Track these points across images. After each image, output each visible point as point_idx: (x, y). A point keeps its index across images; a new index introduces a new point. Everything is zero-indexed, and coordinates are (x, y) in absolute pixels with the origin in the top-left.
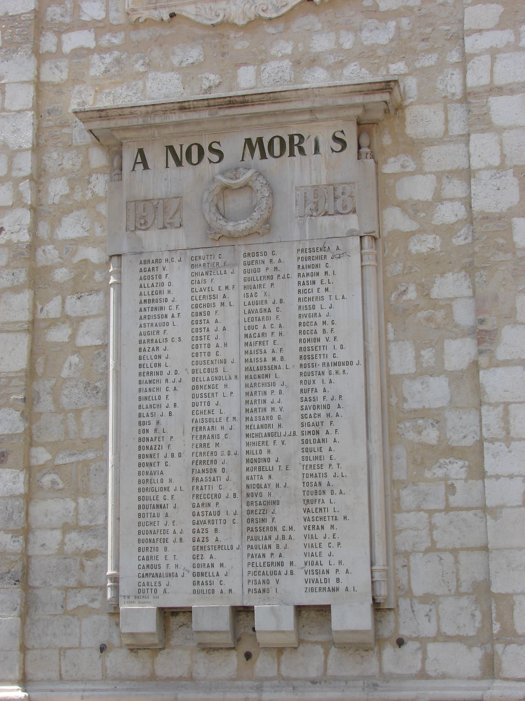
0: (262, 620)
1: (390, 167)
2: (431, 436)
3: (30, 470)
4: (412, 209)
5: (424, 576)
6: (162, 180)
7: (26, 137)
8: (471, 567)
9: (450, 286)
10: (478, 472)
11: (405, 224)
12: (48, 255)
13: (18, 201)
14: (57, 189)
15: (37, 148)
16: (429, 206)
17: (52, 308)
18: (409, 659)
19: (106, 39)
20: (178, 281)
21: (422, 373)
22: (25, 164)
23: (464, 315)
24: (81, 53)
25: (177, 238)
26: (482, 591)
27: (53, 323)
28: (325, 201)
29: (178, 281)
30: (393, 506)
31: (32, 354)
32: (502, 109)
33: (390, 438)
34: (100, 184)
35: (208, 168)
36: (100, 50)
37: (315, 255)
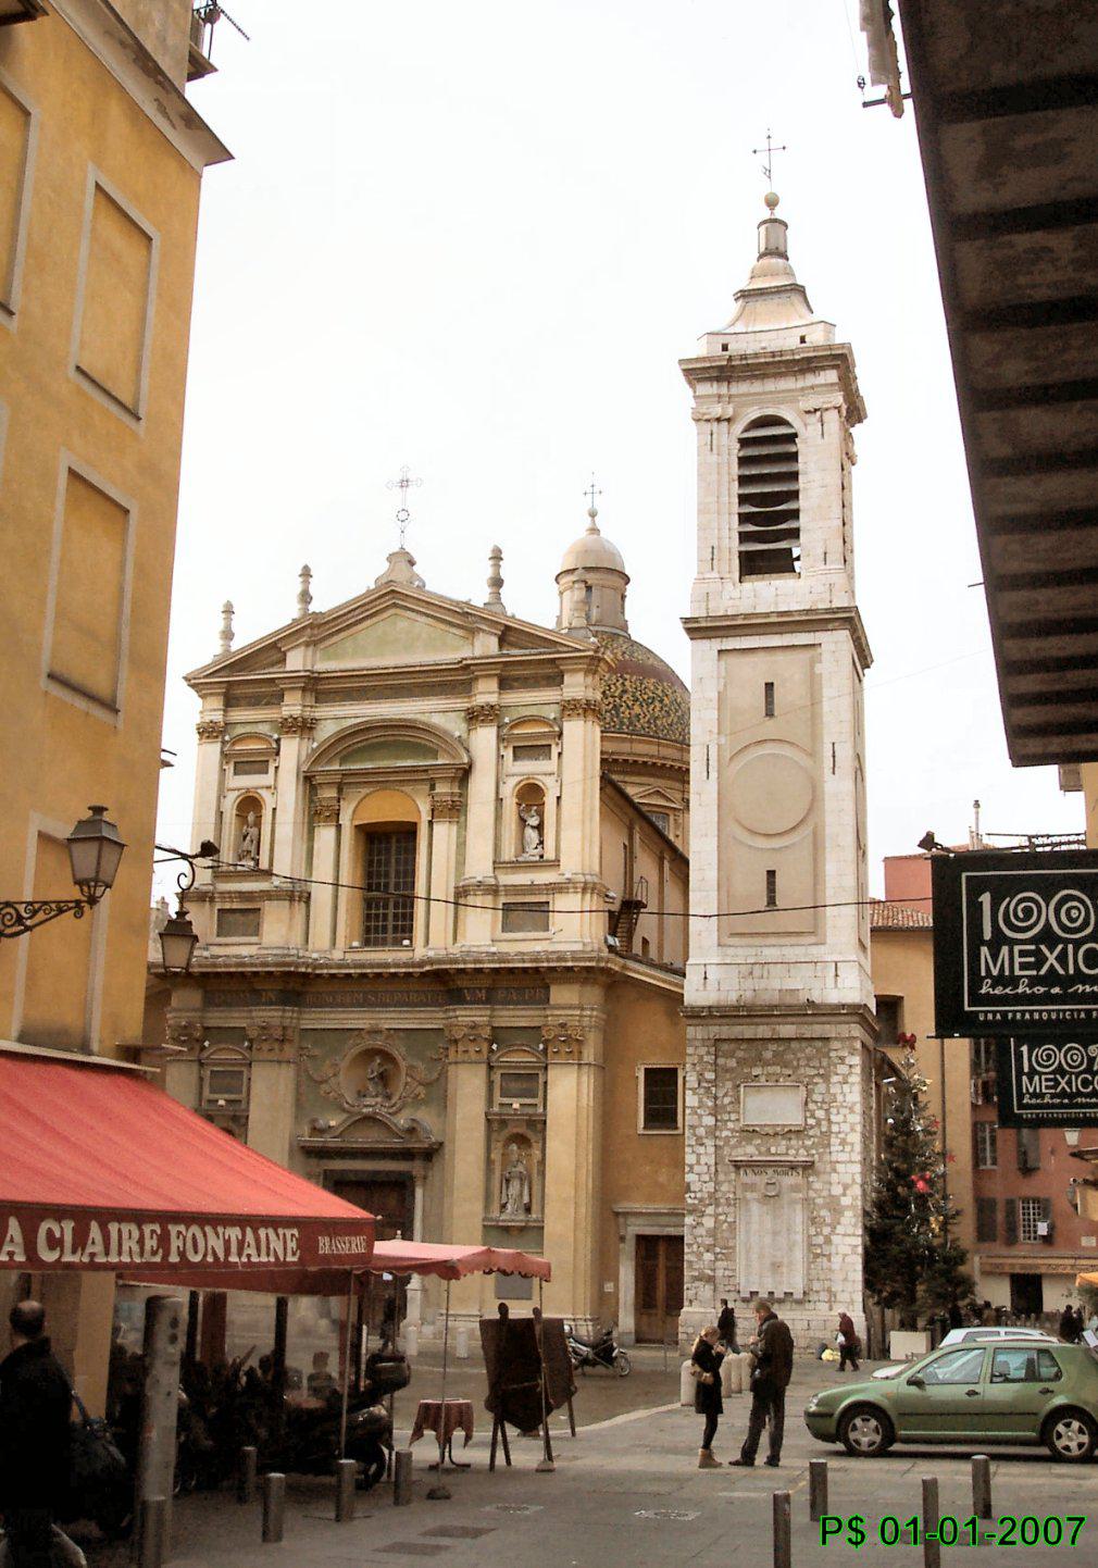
0: (776, 1296)
1: (811, 1179)
2: (819, 1251)
3: (716, 1254)
4: (816, 1191)
5: (816, 1286)
6: (749, 1177)
8: (827, 1284)
9: (824, 1213)
10: (829, 1260)
11: (815, 1195)
13: (711, 1180)
14: (721, 1177)
15: (716, 1164)
16: (821, 1191)
17: (720, 1210)
18: (811, 1306)
20: (755, 1207)
21: (817, 1234)
22: (713, 1169)
24: (727, 1136)
25: (755, 1195)
26: (829, 1290)
27: (721, 1214)
28: (795, 1188)
29: (755, 1207)
30: (809, 1269)
31: (715, 1222)
32: (840, 1167)
33: (809, 1251)
34: (733, 1176)
36: (734, 1137)
37: (793, 1202)
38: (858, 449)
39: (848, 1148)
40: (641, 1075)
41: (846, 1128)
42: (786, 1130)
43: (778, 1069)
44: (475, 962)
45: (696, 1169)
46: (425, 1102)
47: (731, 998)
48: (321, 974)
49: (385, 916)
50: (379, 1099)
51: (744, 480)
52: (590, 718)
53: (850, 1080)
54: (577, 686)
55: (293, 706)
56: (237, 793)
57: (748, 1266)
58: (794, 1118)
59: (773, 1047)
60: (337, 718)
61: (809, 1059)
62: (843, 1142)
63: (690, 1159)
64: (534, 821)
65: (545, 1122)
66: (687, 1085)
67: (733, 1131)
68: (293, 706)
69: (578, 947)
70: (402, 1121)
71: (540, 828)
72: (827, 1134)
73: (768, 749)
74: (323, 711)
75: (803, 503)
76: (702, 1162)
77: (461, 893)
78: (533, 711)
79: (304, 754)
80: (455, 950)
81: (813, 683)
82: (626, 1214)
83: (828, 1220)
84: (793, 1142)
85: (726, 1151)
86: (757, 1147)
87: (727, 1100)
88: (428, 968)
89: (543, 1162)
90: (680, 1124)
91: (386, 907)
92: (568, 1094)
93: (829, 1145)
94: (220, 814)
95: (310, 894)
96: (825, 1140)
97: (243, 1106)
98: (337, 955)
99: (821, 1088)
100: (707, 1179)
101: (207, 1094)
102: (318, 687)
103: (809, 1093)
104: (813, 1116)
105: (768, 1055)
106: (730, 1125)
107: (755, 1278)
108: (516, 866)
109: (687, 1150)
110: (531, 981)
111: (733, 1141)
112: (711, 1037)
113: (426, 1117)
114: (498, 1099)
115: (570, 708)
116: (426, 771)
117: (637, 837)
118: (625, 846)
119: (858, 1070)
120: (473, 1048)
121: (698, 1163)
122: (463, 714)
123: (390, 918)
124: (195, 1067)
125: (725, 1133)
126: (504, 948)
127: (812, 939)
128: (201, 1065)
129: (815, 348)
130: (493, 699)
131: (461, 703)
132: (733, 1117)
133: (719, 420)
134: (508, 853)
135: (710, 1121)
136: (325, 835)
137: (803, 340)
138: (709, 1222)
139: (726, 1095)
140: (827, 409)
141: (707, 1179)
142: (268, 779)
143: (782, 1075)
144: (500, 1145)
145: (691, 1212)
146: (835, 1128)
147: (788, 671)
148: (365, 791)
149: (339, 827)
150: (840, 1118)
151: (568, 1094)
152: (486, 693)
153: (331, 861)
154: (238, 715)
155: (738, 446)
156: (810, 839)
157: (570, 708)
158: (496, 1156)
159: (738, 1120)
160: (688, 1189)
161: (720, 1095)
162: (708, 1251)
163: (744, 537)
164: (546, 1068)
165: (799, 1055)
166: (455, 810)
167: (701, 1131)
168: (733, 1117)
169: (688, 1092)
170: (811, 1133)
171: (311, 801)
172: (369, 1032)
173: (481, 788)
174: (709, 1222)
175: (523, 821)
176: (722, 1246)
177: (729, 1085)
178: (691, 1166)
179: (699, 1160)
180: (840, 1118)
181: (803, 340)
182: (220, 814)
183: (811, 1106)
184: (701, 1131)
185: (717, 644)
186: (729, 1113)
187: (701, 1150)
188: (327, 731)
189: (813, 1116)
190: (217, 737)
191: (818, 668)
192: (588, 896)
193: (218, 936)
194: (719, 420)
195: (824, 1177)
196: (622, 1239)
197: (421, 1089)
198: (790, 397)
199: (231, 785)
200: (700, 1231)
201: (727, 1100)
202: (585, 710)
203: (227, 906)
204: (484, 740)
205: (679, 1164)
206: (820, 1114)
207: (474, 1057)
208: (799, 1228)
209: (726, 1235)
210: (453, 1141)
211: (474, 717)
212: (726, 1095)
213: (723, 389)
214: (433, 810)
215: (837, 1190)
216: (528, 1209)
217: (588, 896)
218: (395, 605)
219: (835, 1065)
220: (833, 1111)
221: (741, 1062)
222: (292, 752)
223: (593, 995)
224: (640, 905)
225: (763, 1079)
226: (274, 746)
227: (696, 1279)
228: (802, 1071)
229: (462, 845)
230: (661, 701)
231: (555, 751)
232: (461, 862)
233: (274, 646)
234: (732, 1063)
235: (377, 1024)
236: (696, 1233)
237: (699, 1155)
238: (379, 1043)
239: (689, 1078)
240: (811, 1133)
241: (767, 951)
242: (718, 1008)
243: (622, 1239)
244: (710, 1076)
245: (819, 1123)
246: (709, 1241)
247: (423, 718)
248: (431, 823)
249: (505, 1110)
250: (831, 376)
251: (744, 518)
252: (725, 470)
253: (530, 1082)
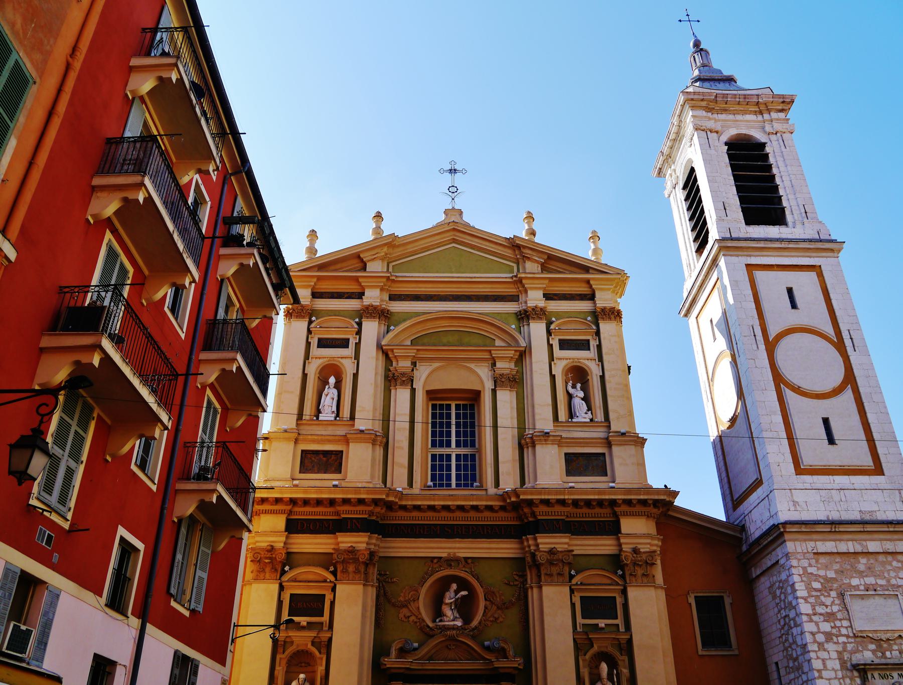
19: (850, 640)
24: (844, 643)
42: (896, 635)
45: (825, 674)
48: (406, 506)
59: (863, 560)
63: (817, 664)
67: (848, 636)
68: (373, 296)
76: (829, 667)
86: (874, 652)
94: (305, 376)
112: (810, 550)
125: (842, 639)
130: (542, 303)
132: (846, 623)
135: (826, 627)
136: (401, 396)
148: (436, 365)
149: (413, 391)
159: (851, 627)
165: (889, 568)
166: (516, 381)
167: (820, 638)
171: (387, 370)
178: (819, 671)
182: (305, 376)
186: (841, 620)
190: (304, 317)
214: (495, 382)
218: (454, 241)
226: (356, 326)
233: (358, 256)
235: (455, 553)
237: (823, 660)
248: (494, 392)
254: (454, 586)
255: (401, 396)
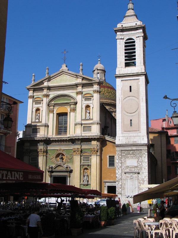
4: (140, 177)
6: (127, 175)
7: (121, 172)
9: (141, 181)
12: (122, 178)
14: (123, 175)
17: (122, 181)
20: (129, 181)
23: (142, 183)
25: (129, 178)
29: (129, 181)
33: (138, 188)
35: (130, 175)
37: (135, 179)
38: (146, 45)
39: (146, 170)
40: (108, 157)
41: (145, 166)
43: (132, 155)
44: (78, 137)
45: (118, 174)
46: (70, 162)
47: (124, 143)
49: (62, 129)
50: (61, 162)
51: (125, 50)
52: (98, 93)
53: (146, 157)
54: (96, 87)
55: (45, 92)
56: (35, 108)
57: (128, 191)
58: (136, 165)
59: (132, 151)
60: (53, 94)
61: (138, 154)
62: (145, 169)
63: (117, 172)
64: (88, 112)
65: (91, 166)
66: (117, 159)
67: (124, 167)
69: (96, 134)
70: (65, 166)
71: (89, 113)
72: (141, 168)
73: (130, 98)
74: (50, 93)
75: (136, 54)
77: (76, 125)
78: (88, 92)
79: (47, 101)
80: (74, 135)
81: (138, 86)
82: (106, 182)
83: (142, 183)
84: (136, 169)
85: (123, 170)
87: (123, 161)
88: (70, 138)
89: (90, 173)
90: (115, 166)
91: (62, 128)
92: (95, 160)
93: (142, 169)
95: (49, 126)
96: (141, 168)
97: (37, 163)
98: (54, 136)
99: (140, 159)
100: (120, 175)
101: (31, 162)
102: (49, 88)
103: (138, 160)
104: (139, 164)
105: (131, 153)
106: (124, 166)
107: (129, 193)
108: (85, 120)
109: (117, 170)
110: (88, 140)
111: (125, 169)
113: (70, 165)
114: (82, 162)
115: (95, 91)
116: (69, 103)
117: (107, 115)
118: (105, 117)
119: (147, 155)
120: (78, 152)
121: (118, 172)
122: (76, 93)
123: (63, 129)
124: (28, 157)
125: (123, 167)
126: (83, 135)
127: (138, 132)
128: (30, 156)
129: (139, 25)
131: (75, 91)
132: (125, 164)
133: (121, 39)
134: (84, 118)
135: (120, 165)
137: (136, 24)
138: (120, 183)
139: (123, 160)
140: (141, 37)
141: (120, 175)
142: (41, 105)
143: (133, 156)
144: (83, 170)
145: (117, 182)
146: (143, 166)
147: (133, 84)
148: (58, 107)
149: (53, 113)
150: (144, 164)
151: (95, 160)
152: (80, 89)
153: (52, 121)
154: (35, 94)
155: (124, 44)
156: (138, 114)
157: (95, 91)
158: (82, 172)
160: (117, 177)
161: (122, 160)
162: (120, 188)
163: (126, 60)
164: (91, 156)
165: (137, 153)
166: (74, 110)
167: (119, 167)
168: (125, 164)
169: (117, 160)
170: (139, 167)
172: (59, 150)
173: (79, 106)
174: (120, 183)
175: (86, 112)
176: (122, 188)
177: (124, 158)
178: (117, 173)
179: (118, 172)
180: (144, 164)
181: (136, 24)
183: (139, 162)
184: (119, 167)
185: (121, 79)
187: (119, 170)
188: (51, 96)
189: (139, 164)
191: (139, 83)
192: (98, 125)
193: (32, 133)
194: (121, 39)
195: (141, 175)
196: (105, 187)
197: (69, 160)
198: (134, 34)
199: (35, 106)
200: (119, 185)
201: (123, 161)
202: (97, 92)
203: (34, 128)
204: (79, 98)
205: (115, 173)
206: (140, 163)
207: (78, 154)
208: (137, 184)
209: (124, 185)
210: (74, 169)
211: (77, 93)
212: (123, 160)
213: (122, 33)
215: (144, 177)
216: (88, 181)
217: (98, 125)
218: (63, 74)
219: (143, 155)
220: (143, 163)
221: (126, 154)
222: (45, 100)
223: (98, 143)
224: (108, 127)
225: (130, 157)
227: (119, 194)
228: (137, 156)
229: (75, 116)
230: (111, 93)
231: (92, 99)
232: (75, 120)
234: (124, 154)
236: (118, 185)
238: (61, 152)
239: (116, 157)
240: (139, 167)
241: (130, 134)
242: (122, 144)
243: (105, 187)
244: (120, 157)
245: (140, 165)
246: (121, 187)
247: (69, 94)
249: (84, 163)
250: (141, 30)
251: (126, 57)
252: (122, 48)
253: (88, 158)
254: (61, 155)
255: (51, 115)
